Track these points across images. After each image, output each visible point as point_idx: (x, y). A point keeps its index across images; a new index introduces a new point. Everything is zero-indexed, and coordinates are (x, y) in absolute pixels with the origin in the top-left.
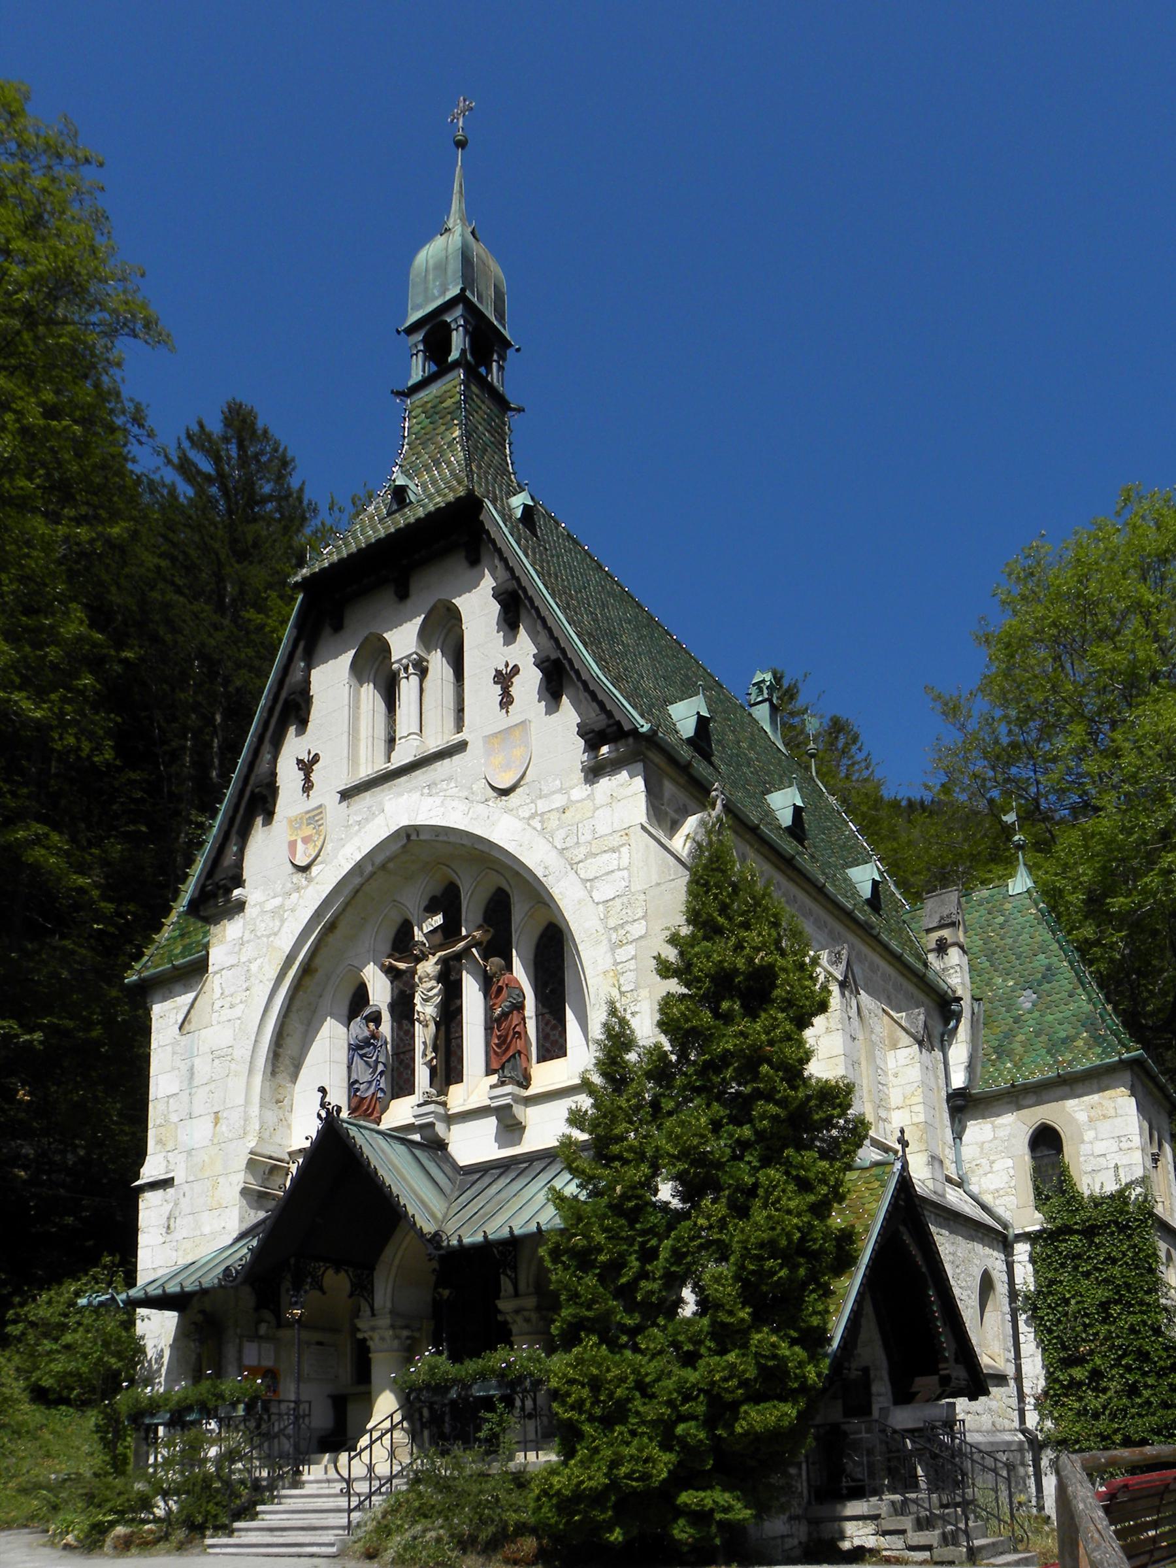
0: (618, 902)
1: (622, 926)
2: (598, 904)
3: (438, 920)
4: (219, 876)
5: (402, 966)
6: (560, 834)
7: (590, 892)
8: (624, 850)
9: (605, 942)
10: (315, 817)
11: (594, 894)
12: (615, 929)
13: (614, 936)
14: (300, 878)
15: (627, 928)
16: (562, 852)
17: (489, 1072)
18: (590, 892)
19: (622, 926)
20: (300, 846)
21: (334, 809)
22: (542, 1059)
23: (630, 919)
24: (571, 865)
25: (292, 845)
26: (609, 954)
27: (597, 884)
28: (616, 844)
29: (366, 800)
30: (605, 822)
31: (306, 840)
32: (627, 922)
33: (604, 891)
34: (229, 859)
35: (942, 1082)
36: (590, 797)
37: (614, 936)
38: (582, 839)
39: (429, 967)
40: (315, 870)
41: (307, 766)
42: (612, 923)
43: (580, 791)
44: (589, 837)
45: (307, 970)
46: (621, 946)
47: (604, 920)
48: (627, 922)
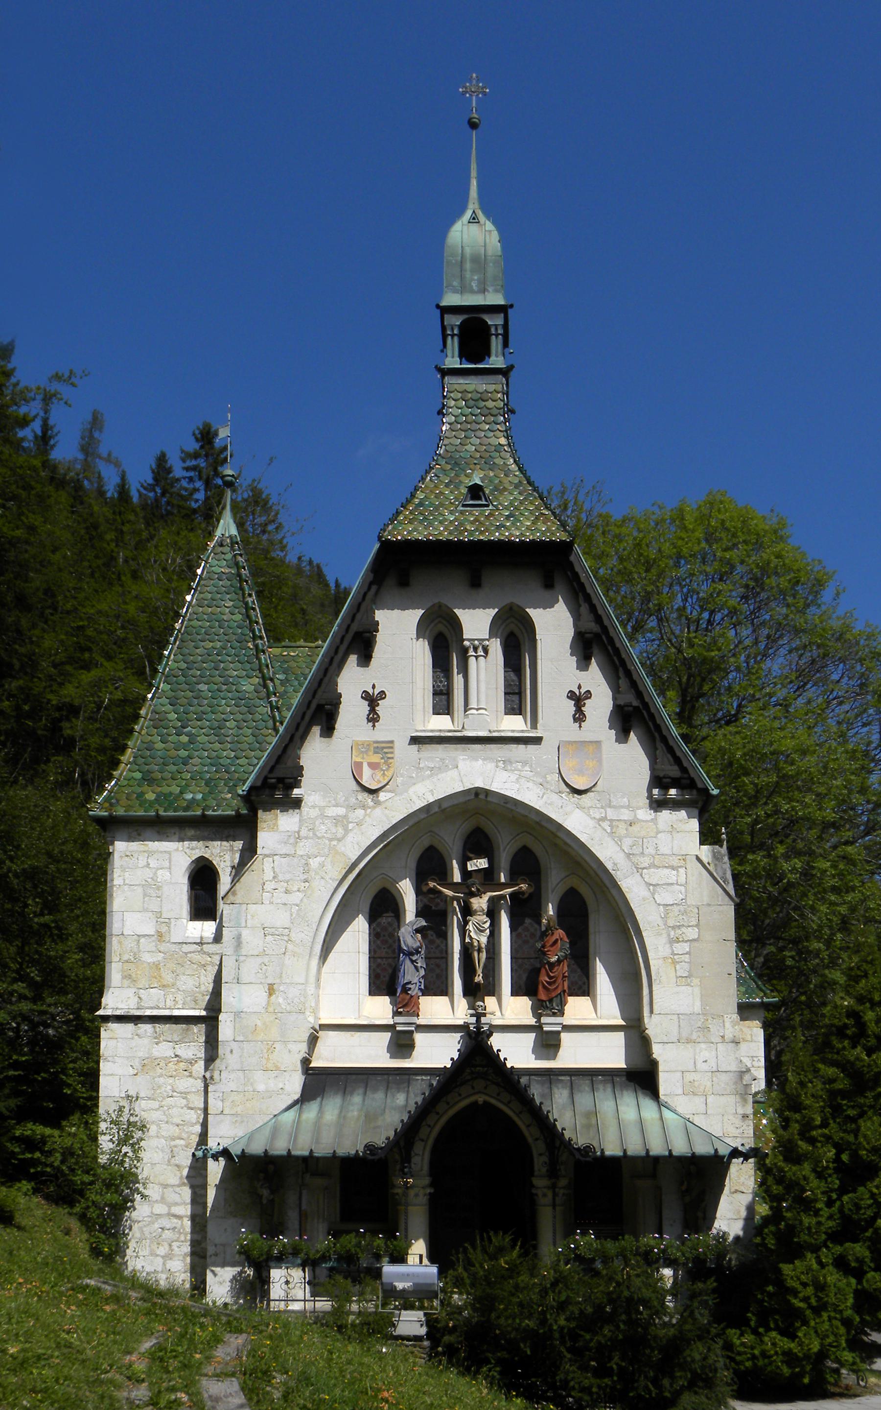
0: (676, 908)
1: (679, 927)
2: (659, 905)
6: (627, 843)
7: (653, 894)
8: (682, 870)
9: (665, 935)
11: (656, 897)
12: (673, 928)
13: (672, 933)
15: (684, 929)
18: (653, 894)
19: (679, 927)
23: (685, 924)
24: (637, 868)
26: (668, 946)
27: (658, 889)
28: (675, 864)
30: (665, 843)
32: (683, 925)
33: (665, 897)
36: (654, 821)
37: (672, 933)
38: (646, 851)
42: (671, 923)
43: (645, 814)
44: (651, 850)
46: (678, 942)
47: (665, 918)
48: (683, 925)
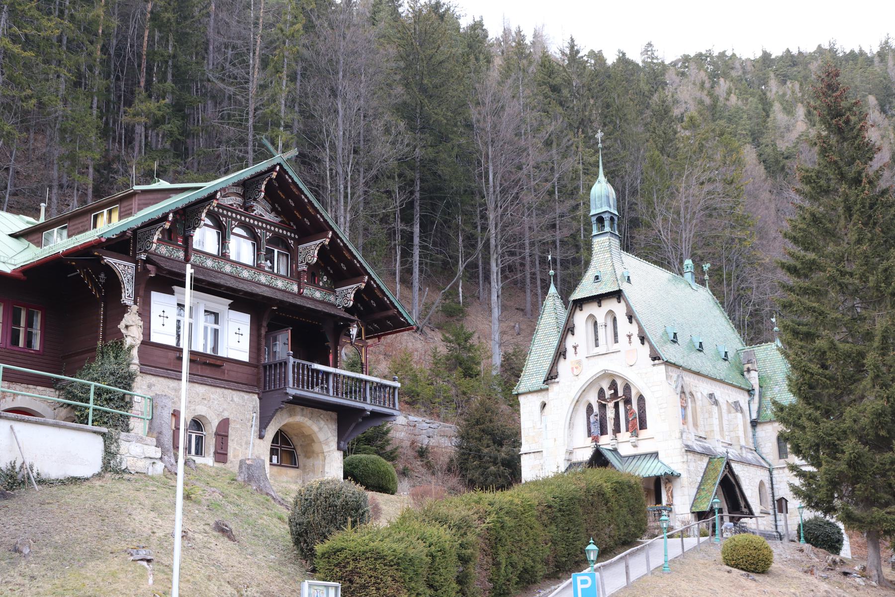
3: (612, 391)
4: (552, 375)
5: (603, 402)
10: (579, 362)
14: (576, 378)
16: (646, 384)
17: (627, 430)
20: (575, 370)
21: (585, 361)
22: (640, 429)
25: (572, 368)
29: (593, 360)
31: (576, 368)
34: (554, 371)
35: (748, 418)
39: (611, 405)
40: (579, 376)
41: (575, 348)
45: (577, 401)
